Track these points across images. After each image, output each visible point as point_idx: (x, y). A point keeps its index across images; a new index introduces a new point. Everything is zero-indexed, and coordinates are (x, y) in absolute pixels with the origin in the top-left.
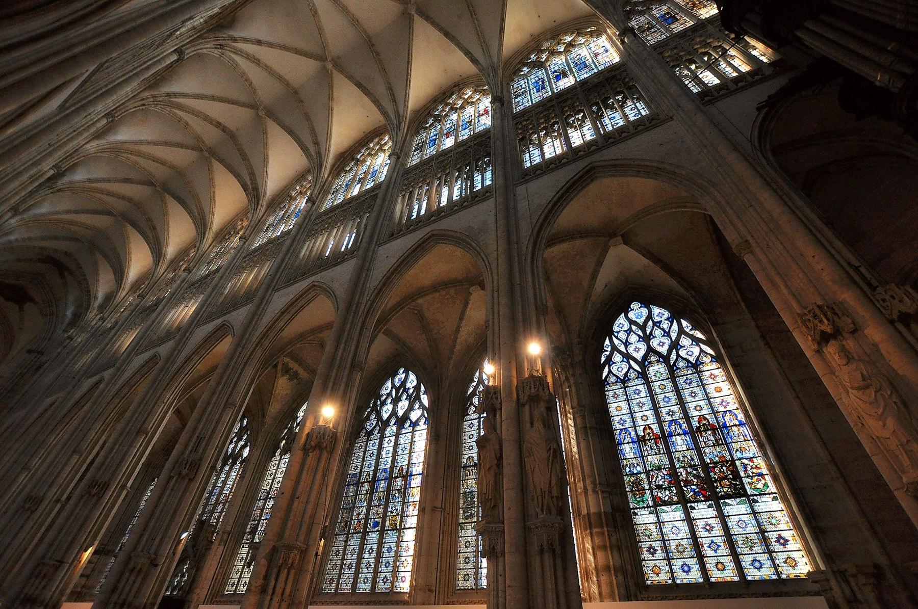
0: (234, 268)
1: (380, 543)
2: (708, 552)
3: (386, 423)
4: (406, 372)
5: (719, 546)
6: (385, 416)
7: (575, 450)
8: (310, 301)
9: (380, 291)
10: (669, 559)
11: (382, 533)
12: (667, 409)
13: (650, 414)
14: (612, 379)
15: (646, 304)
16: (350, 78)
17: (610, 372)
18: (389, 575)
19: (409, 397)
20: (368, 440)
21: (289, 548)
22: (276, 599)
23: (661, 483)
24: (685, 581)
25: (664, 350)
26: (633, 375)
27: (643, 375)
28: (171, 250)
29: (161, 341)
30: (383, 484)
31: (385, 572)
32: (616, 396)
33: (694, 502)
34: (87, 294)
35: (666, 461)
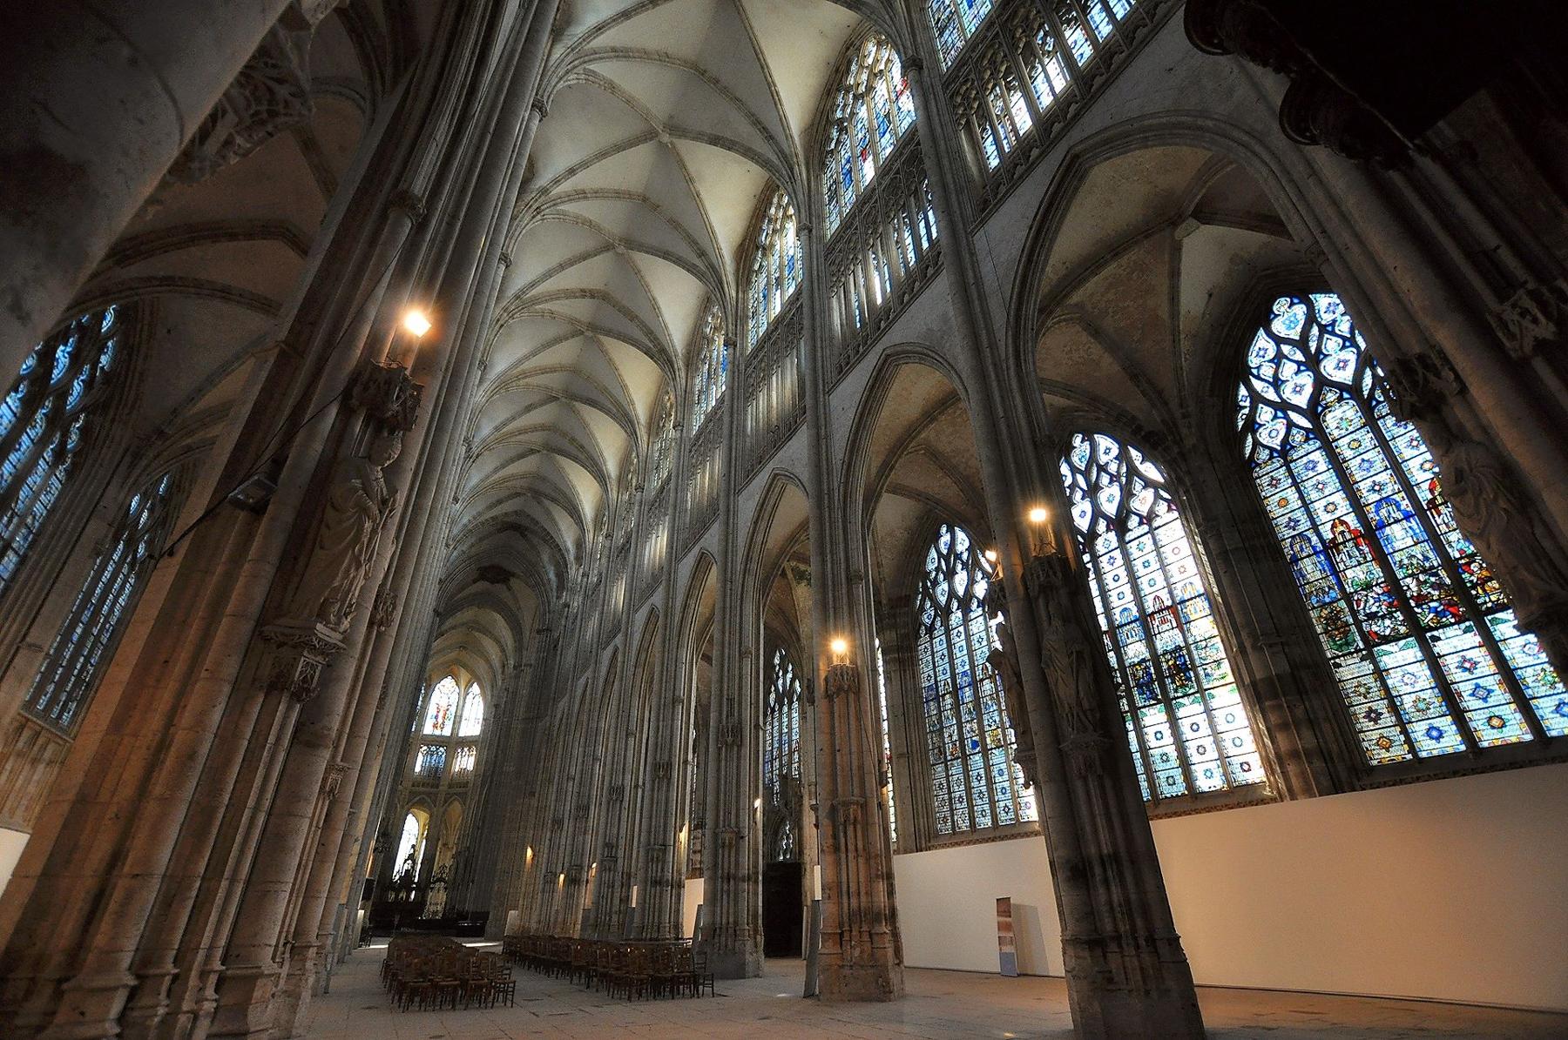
0: (685, 472)
1: (988, 767)
2: (1470, 703)
3: (946, 612)
4: (951, 531)
5: (1489, 692)
6: (943, 600)
7: (1216, 590)
8: (781, 494)
9: (849, 466)
10: (1402, 724)
11: (985, 753)
12: (1369, 482)
13: (1340, 499)
14: (1264, 455)
15: (1301, 293)
16: (699, 137)
17: (1256, 443)
18: (1009, 803)
19: (965, 565)
20: (932, 639)
21: (846, 804)
22: (851, 856)
23: (1374, 609)
24: (1435, 753)
25: (1346, 376)
26: (1298, 437)
27: (1318, 432)
28: (611, 467)
29: (651, 589)
30: (968, 693)
31: (1003, 801)
32: (1274, 483)
33: (1436, 629)
34: (558, 550)
35: (1378, 572)
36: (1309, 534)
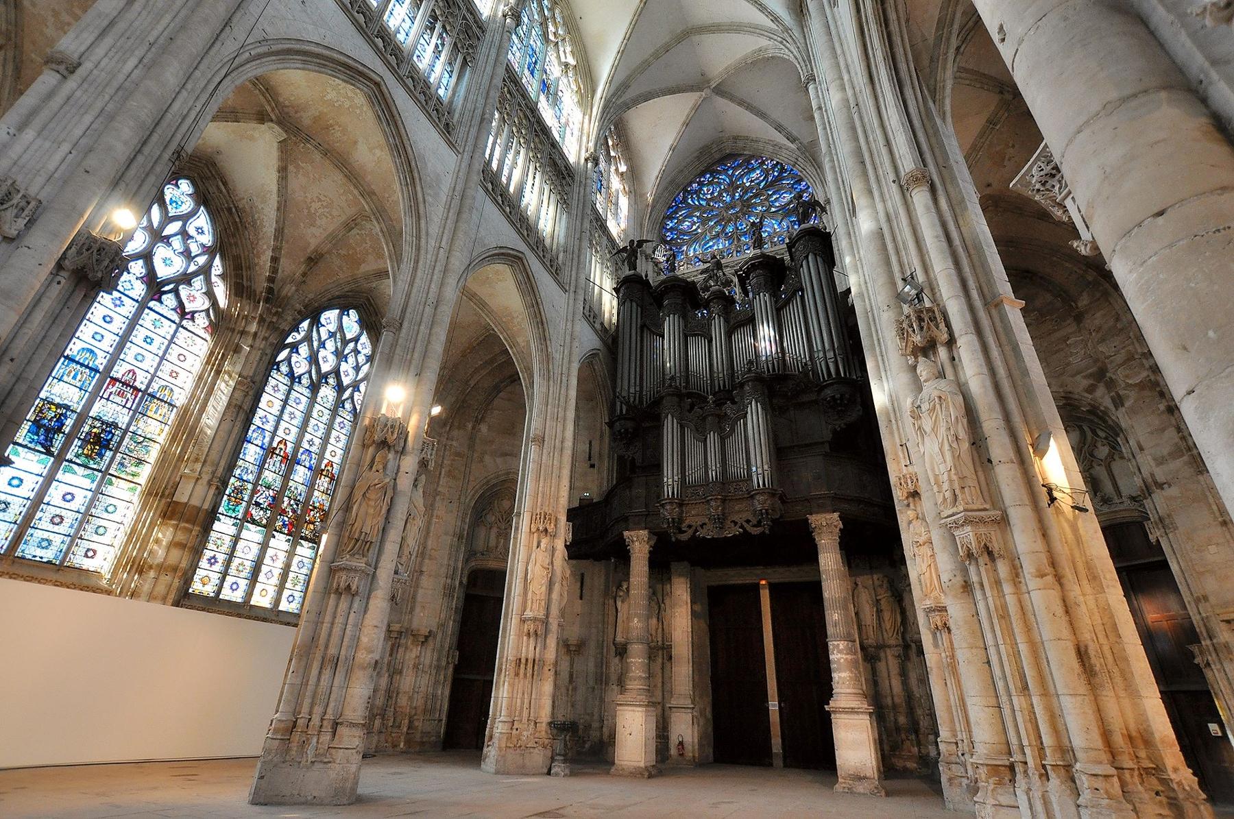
10: (224, 574)
13: (294, 431)
25: (346, 381)
35: (278, 485)
36: (267, 434)
